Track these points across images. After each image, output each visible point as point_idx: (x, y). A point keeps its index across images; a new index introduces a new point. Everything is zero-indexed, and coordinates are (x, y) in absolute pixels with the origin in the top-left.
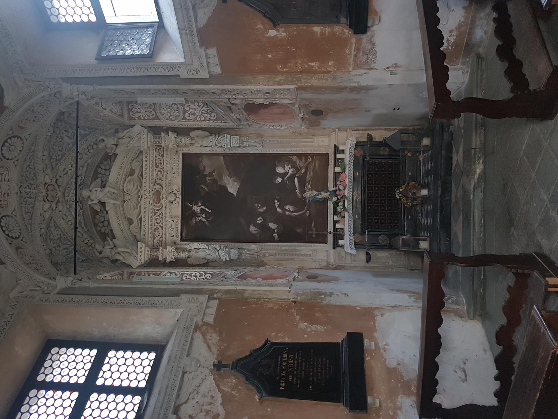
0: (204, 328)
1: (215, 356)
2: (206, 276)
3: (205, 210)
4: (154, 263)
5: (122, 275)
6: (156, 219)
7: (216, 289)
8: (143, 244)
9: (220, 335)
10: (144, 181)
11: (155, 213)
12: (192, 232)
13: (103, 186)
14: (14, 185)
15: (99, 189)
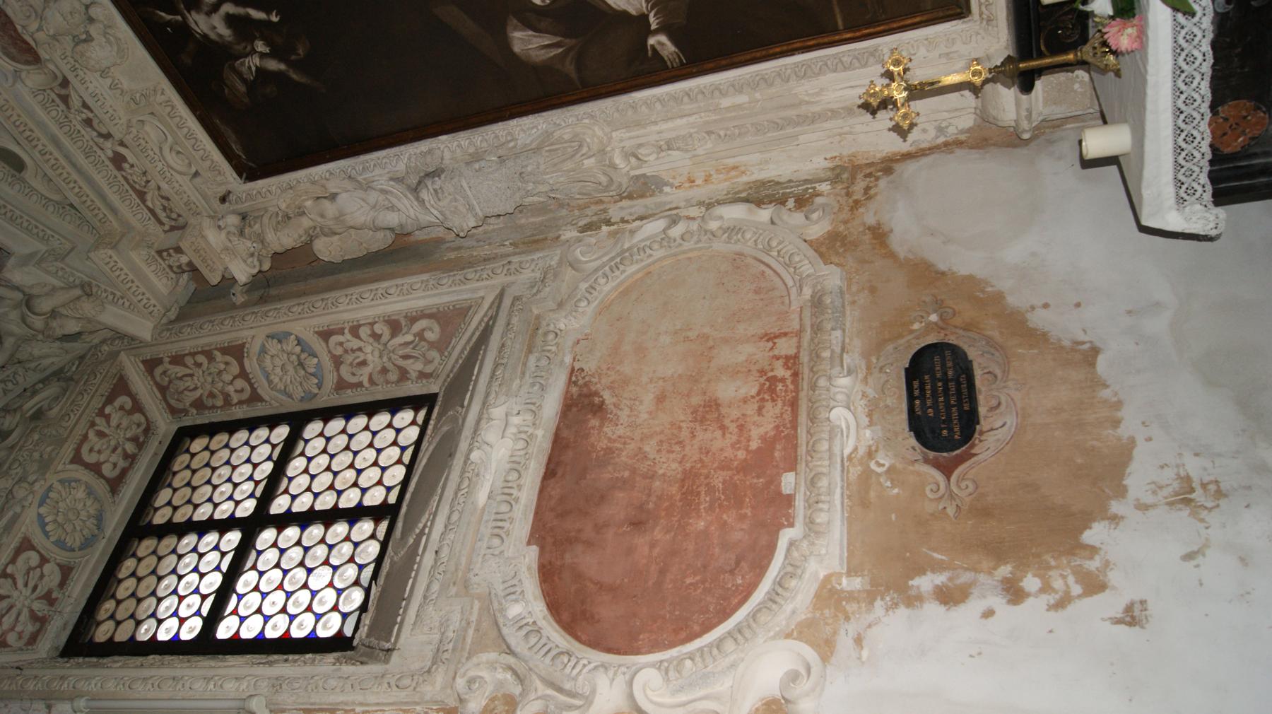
3: (248, 18)
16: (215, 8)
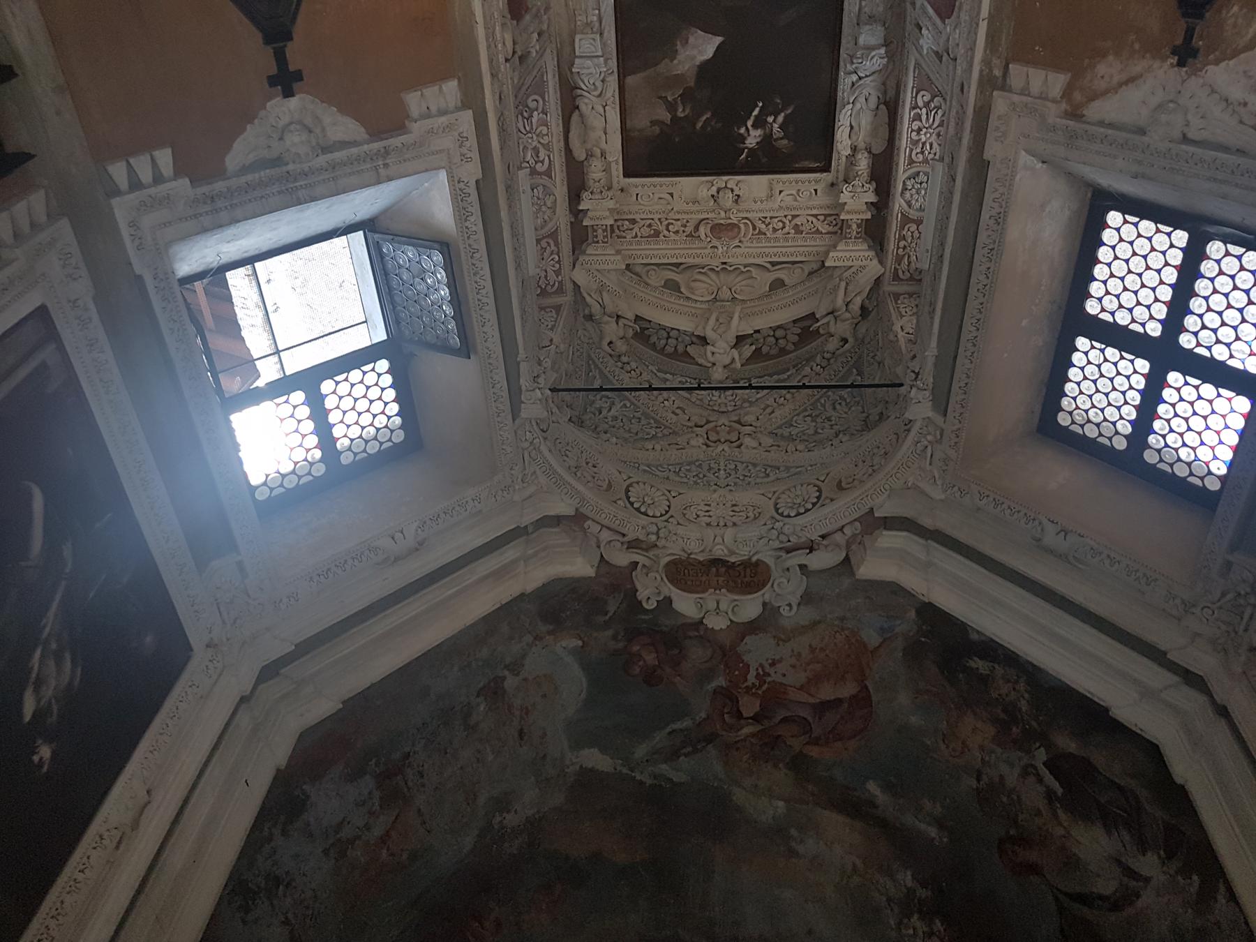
0: (1078, 96)
1: (1157, 64)
2: (920, 104)
4: (875, 232)
5: (897, 296)
6: (775, 230)
7: (981, 71)
8: (831, 254)
9: (1103, 55)
10: (691, 261)
11: (761, 233)
12: (809, 146)
13: (704, 340)
14: (715, 496)
15: (709, 348)
16: (747, 129)
